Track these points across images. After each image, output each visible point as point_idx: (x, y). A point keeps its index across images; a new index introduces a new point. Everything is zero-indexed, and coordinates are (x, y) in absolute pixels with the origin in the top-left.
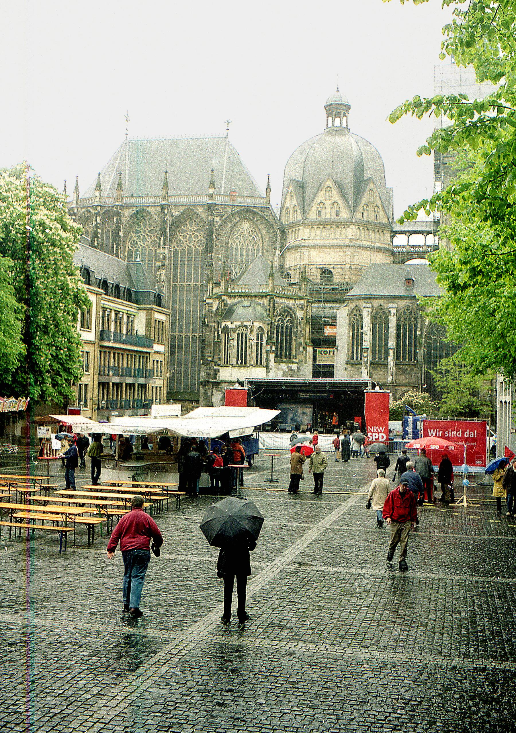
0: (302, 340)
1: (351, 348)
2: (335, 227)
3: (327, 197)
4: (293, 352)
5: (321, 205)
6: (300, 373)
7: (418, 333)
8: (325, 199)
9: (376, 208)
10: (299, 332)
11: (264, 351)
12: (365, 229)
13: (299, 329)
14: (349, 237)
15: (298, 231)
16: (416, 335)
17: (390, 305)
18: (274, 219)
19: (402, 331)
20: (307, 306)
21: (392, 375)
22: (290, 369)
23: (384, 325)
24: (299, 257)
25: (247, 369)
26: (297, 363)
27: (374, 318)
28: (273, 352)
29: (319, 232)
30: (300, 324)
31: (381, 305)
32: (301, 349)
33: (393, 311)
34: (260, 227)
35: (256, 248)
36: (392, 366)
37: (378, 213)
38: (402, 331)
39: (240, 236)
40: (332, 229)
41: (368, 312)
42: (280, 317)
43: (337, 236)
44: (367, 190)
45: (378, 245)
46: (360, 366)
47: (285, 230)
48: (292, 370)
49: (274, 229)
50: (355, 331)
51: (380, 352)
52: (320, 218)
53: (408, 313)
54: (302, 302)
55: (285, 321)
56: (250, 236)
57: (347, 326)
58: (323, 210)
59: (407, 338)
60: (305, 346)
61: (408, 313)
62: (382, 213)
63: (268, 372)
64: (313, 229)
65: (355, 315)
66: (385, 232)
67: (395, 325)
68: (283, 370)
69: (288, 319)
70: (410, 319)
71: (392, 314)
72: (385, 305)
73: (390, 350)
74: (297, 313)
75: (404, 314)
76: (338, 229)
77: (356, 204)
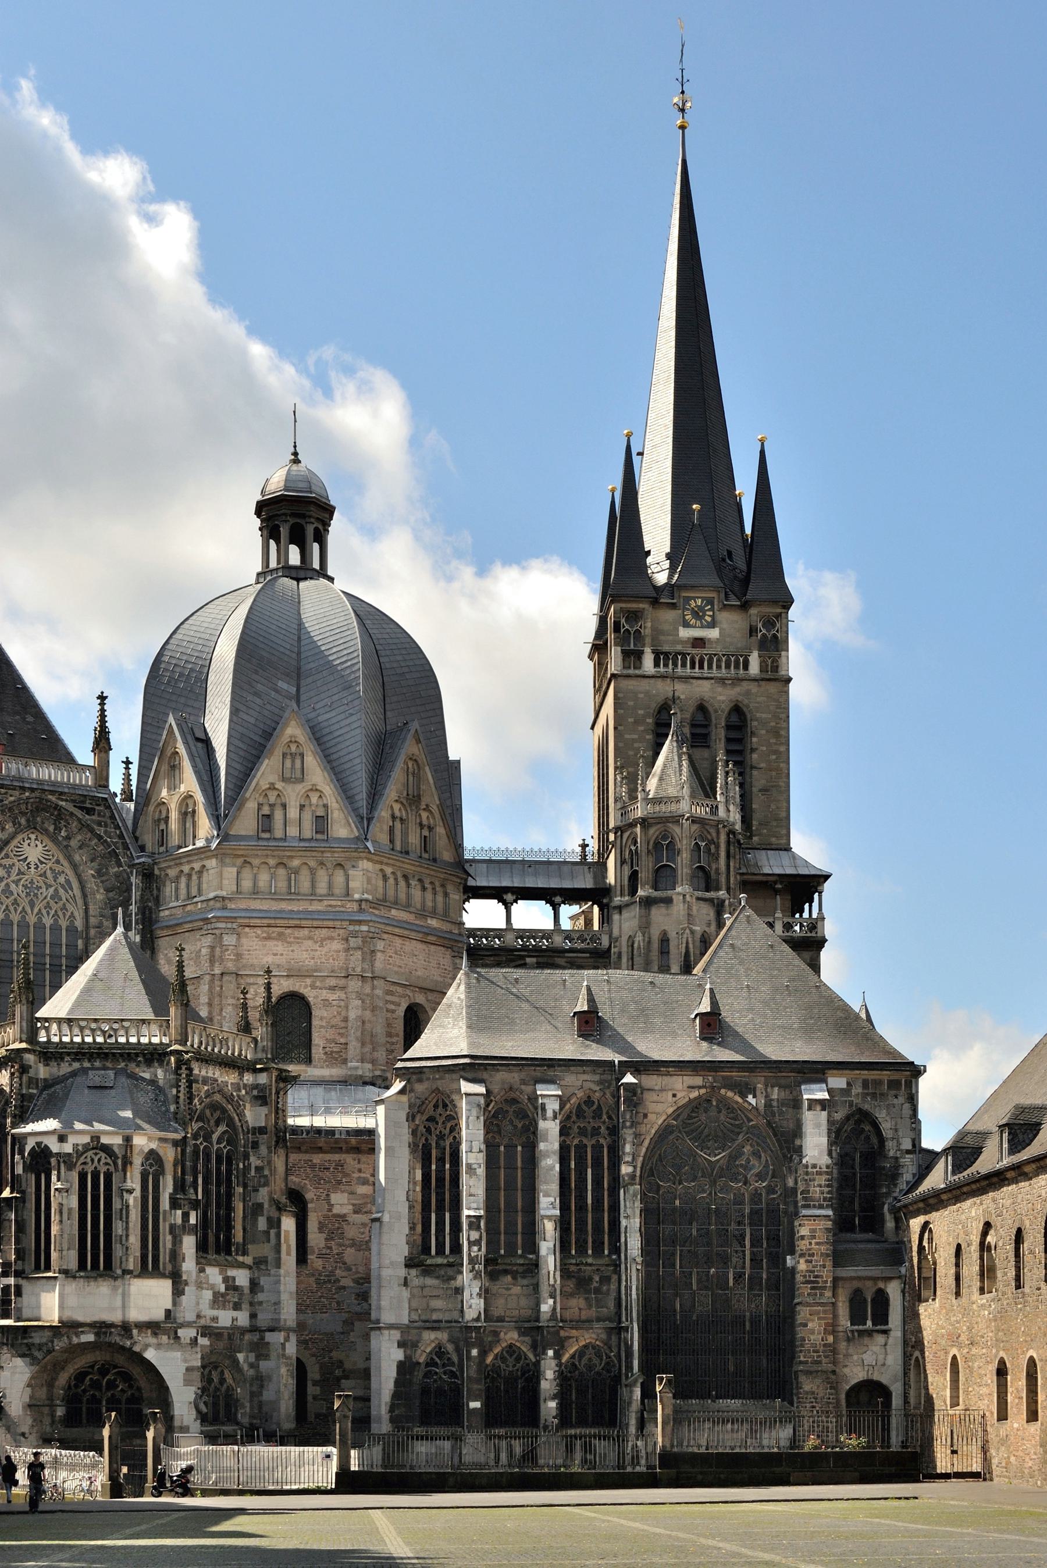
0: (263, 1195)
1: (418, 1216)
2: (312, 863)
3: (288, 775)
4: (238, 1235)
5: (272, 797)
6: (260, 1297)
7: (625, 1170)
8: (283, 781)
9: (424, 815)
10: (253, 1173)
11: (164, 1228)
12: (399, 874)
13: (254, 1161)
14: (357, 896)
15: (200, 873)
16: (616, 1181)
17: (542, 1090)
18: (121, 836)
19: (573, 1166)
20: (277, 1093)
21: (552, 1296)
22: (231, 1285)
23: (519, 1148)
24: (204, 951)
25: (111, 1282)
26: (250, 1268)
27: (493, 1126)
28: (193, 1230)
29: (264, 878)
30: (255, 1145)
31: (511, 1089)
32: (262, 1224)
33: (552, 1106)
34: (77, 858)
35: (64, 923)
36: (552, 1268)
37: (430, 829)
38: (573, 1166)
39: (17, 882)
40: (305, 873)
41: (479, 1106)
42: (201, 1124)
43: (322, 888)
44: (402, 758)
45: (433, 923)
46: (450, 1272)
47: (156, 872)
48: (236, 1288)
49: (119, 865)
50: (434, 1167)
51: (511, 1224)
52: (266, 835)
53: (589, 1112)
54: (263, 1079)
55: (215, 1137)
56: (48, 886)
57: (406, 1151)
58: (278, 815)
59: (589, 1187)
60: (274, 1214)
61: (589, 1112)
62: (440, 830)
63: (178, 1292)
64: (247, 874)
65: (431, 1119)
66: (450, 888)
67: (556, 1146)
68: (212, 1287)
69: (222, 1128)
70: (596, 1132)
71: (549, 1113)
72: (523, 1087)
73: (546, 1221)
74: (247, 1113)
75: (578, 1116)
76: (322, 875)
77: (375, 795)
